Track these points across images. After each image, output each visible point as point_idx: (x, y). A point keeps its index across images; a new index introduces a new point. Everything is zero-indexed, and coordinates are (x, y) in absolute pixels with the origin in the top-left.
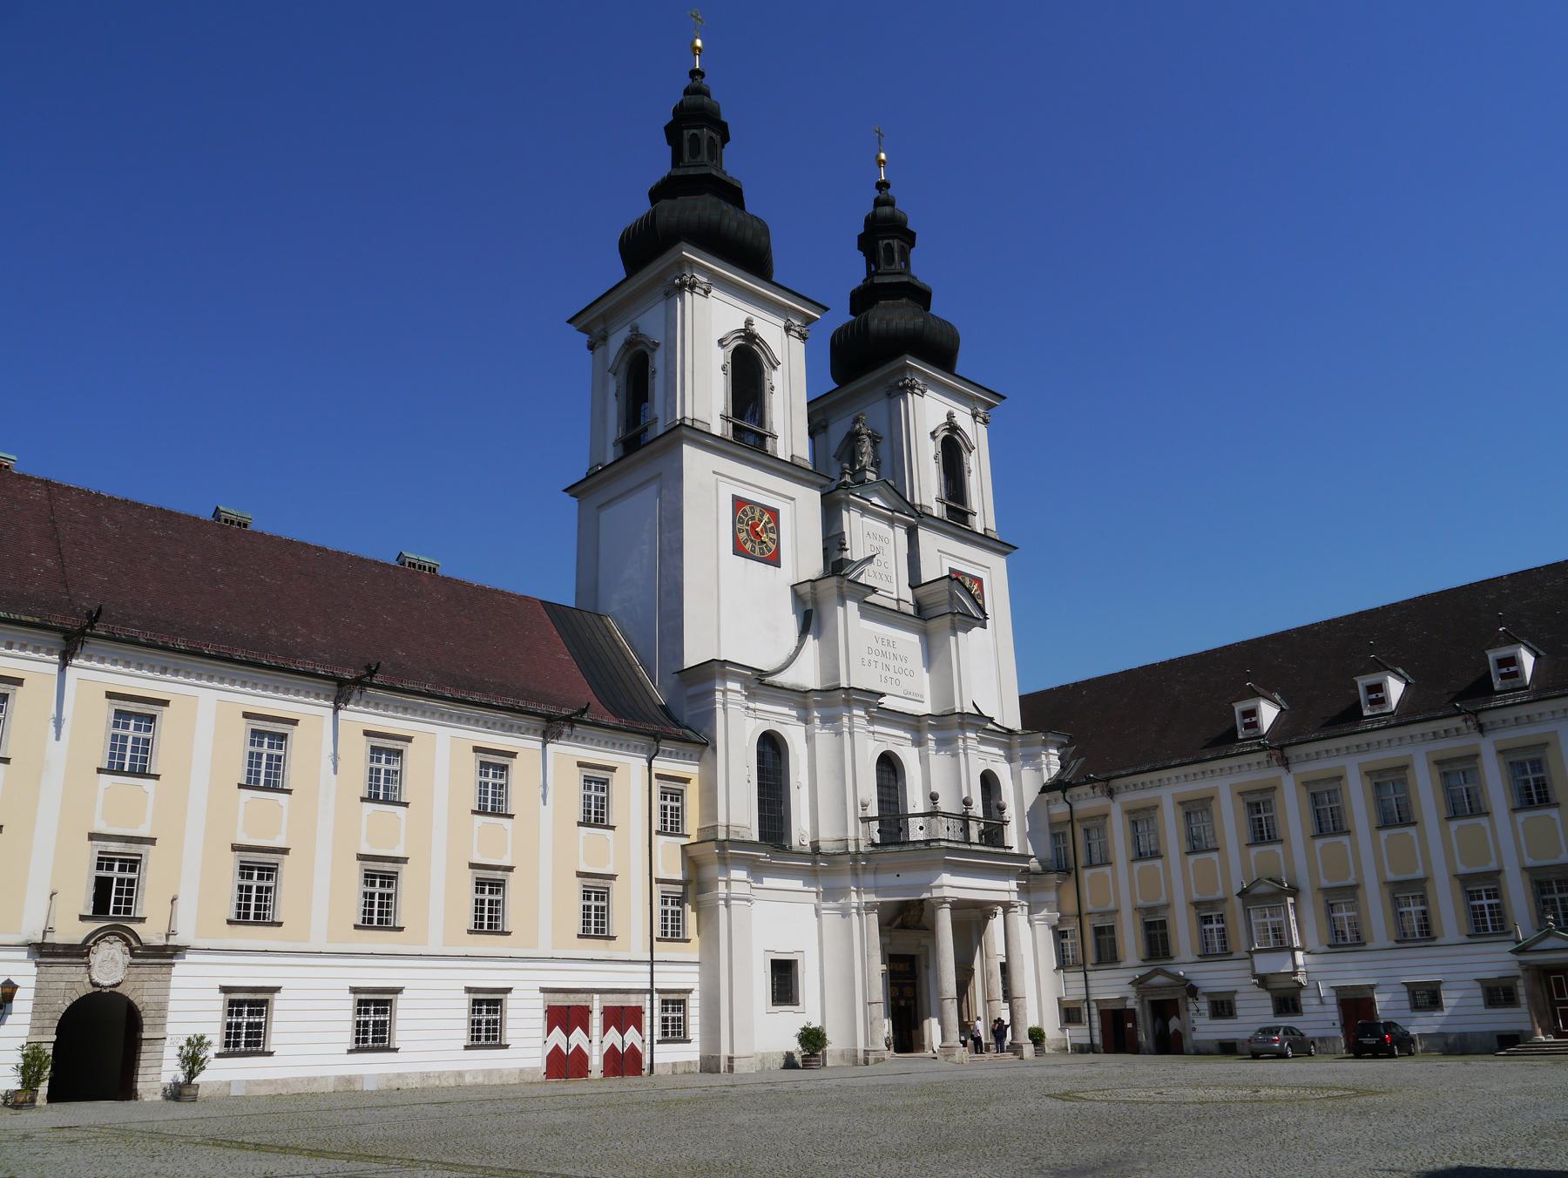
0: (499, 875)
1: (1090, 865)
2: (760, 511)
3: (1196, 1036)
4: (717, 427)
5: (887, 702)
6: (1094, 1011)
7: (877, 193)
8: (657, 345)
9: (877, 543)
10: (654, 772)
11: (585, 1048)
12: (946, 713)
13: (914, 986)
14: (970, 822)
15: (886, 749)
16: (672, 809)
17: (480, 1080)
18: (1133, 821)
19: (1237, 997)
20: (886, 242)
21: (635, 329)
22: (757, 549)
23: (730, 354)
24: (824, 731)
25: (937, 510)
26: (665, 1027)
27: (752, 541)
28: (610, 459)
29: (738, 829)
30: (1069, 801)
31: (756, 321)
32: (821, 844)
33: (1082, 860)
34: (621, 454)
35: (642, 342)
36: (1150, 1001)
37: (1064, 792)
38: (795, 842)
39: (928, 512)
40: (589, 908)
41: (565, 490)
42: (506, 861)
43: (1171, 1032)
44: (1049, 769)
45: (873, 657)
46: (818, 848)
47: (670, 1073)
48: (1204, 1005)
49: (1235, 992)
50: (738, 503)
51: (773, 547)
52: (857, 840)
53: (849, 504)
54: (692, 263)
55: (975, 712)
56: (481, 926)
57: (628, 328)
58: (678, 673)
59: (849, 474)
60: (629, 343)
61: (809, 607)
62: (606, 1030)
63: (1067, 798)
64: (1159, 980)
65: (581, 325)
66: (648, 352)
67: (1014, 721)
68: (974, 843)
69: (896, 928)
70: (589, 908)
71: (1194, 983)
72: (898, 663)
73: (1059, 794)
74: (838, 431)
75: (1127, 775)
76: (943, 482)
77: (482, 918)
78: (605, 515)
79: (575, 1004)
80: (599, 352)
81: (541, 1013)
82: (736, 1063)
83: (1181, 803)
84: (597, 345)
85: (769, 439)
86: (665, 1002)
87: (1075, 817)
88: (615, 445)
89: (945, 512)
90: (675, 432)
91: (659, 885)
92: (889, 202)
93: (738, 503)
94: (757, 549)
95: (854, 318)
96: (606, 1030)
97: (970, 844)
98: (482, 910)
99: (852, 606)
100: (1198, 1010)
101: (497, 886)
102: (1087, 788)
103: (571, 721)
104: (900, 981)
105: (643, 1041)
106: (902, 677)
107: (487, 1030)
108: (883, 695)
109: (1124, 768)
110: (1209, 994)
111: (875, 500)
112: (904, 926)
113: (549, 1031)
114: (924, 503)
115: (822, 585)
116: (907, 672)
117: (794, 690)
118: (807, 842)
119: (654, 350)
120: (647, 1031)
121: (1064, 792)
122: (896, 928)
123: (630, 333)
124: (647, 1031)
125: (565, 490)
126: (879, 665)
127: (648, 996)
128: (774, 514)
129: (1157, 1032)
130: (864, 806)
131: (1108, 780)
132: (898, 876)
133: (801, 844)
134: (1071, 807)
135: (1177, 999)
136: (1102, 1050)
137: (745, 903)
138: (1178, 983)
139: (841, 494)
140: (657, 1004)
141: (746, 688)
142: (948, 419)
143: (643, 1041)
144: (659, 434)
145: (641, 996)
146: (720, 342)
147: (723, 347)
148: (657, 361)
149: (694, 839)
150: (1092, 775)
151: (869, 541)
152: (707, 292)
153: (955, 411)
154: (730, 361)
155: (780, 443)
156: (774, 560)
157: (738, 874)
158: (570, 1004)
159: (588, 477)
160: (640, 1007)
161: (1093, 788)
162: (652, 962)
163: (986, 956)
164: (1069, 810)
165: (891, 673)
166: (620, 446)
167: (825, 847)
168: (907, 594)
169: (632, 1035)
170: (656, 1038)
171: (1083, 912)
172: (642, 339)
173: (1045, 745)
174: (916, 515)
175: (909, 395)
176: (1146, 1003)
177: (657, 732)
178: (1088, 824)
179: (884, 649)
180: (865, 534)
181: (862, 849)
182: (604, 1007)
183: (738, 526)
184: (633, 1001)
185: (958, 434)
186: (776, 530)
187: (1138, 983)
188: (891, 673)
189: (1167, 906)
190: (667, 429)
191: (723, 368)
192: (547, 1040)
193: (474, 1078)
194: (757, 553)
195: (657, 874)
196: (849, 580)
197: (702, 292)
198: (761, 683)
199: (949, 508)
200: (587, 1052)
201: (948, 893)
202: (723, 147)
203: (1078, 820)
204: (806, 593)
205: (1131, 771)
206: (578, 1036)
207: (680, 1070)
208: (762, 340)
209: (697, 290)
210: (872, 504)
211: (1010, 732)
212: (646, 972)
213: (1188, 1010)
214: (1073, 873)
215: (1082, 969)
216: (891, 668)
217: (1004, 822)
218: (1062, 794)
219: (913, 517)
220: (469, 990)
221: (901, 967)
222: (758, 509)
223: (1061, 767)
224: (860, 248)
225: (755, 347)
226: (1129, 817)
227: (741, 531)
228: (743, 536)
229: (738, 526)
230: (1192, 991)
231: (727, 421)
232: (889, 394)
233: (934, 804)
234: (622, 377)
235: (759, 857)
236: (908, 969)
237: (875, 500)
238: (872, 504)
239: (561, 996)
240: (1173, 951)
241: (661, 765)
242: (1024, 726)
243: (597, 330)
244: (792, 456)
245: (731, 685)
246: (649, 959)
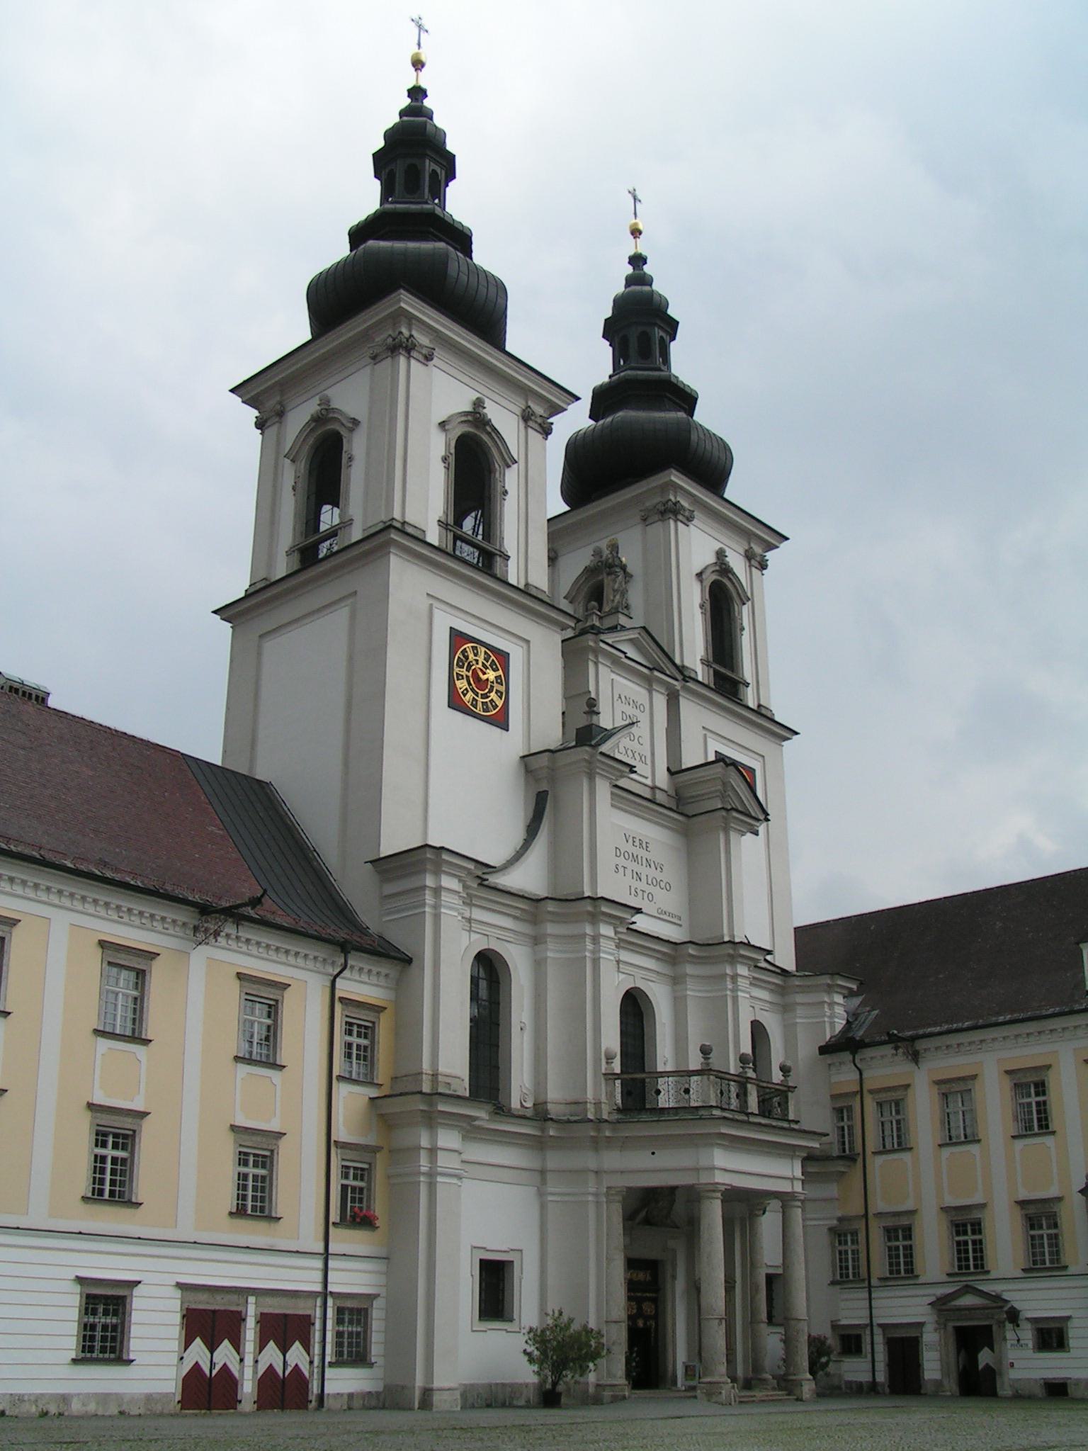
0: (128, 1123)
1: (884, 1151)
2: (486, 653)
3: (1013, 1374)
4: (433, 536)
5: (641, 923)
6: (879, 1338)
7: (630, 270)
8: (356, 422)
9: (630, 710)
10: (338, 994)
11: (234, 1368)
12: (710, 942)
13: (655, 1301)
14: (749, 1086)
15: (632, 986)
16: (358, 1046)
17: (92, 1407)
18: (943, 1094)
19: (1070, 1324)
20: (640, 329)
21: (325, 402)
22: (480, 705)
23: (453, 444)
25: (701, 673)
26: (339, 1345)
27: (473, 690)
28: (281, 572)
29: (448, 1080)
30: (859, 1065)
31: (488, 403)
32: (549, 1106)
33: (871, 1147)
34: (296, 566)
35: (336, 419)
36: (958, 1330)
37: (854, 1053)
38: (515, 1104)
39: (693, 675)
40: (245, 1177)
41: (215, 612)
42: (138, 1105)
43: (980, 1367)
44: (832, 1024)
46: (546, 1112)
47: (345, 1407)
48: (1027, 1335)
49: (1069, 1318)
50: (458, 638)
51: (500, 703)
52: (598, 1104)
53: (597, 652)
55: (746, 941)
56: (101, 1192)
57: (316, 400)
58: (371, 862)
59: (597, 615)
60: (318, 420)
61: (544, 787)
62: (262, 1346)
63: (857, 1061)
64: (968, 1300)
65: (249, 396)
66: (343, 432)
67: (786, 958)
68: (752, 1114)
69: (639, 1224)
70: (245, 1177)
71: (1017, 1305)
72: (652, 872)
73: (847, 1056)
74: (577, 562)
75: (940, 1034)
76: (710, 638)
77: (102, 1181)
78: (269, 645)
79: (222, 1308)
80: (272, 431)
81: (177, 1318)
82: (436, 1398)
83: (1009, 1072)
84: (268, 424)
85: (498, 559)
86: (340, 1311)
87: (866, 1087)
88: (288, 554)
89: (712, 678)
90: (381, 539)
91: (339, 1151)
92: (646, 280)
93: (458, 638)
94: (480, 705)
95: (592, 422)
96: (262, 1346)
97: (748, 1114)
98: (103, 1171)
99: (603, 790)
100: (1018, 1340)
101: (126, 1140)
102: (888, 1050)
103: (234, 914)
104: (639, 1294)
105: (311, 1362)
106: (656, 891)
107: (104, 1339)
108: (639, 911)
109: (935, 1025)
110: (1034, 1321)
111: (632, 653)
112: (648, 1222)
113: (188, 1344)
114: (687, 663)
115: (563, 759)
116: (663, 885)
117: (523, 897)
118: (529, 1104)
119: (351, 430)
120: (317, 1349)
121: (854, 1053)
122: (639, 1224)
123: (319, 408)
124: (317, 1349)
125: (215, 612)
126: (628, 872)
127: (319, 1302)
128: (502, 659)
129: (961, 1367)
130: (609, 1058)
131: (913, 1039)
132: (653, 1153)
133: (522, 1106)
134: (861, 1074)
135: (989, 1328)
136: (887, 1390)
137: (455, 1181)
138: (995, 1305)
139: (590, 641)
140: (330, 1313)
141: (465, 887)
142: (718, 558)
143: (311, 1362)
144: (354, 540)
145: (310, 1302)
146: (442, 425)
147: (445, 430)
148: (357, 447)
149: (385, 1091)
150: (895, 1032)
151: (620, 707)
152: (428, 358)
153: (727, 549)
154: (453, 451)
155: (512, 564)
156: (501, 720)
157: (448, 1138)
158: (217, 1308)
159: (248, 595)
160: (309, 1316)
161: (896, 1048)
162: (326, 1255)
163: (752, 1264)
164: (858, 1077)
165: (642, 885)
166: (296, 556)
167: (553, 1110)
168: (662, 779)
169: (297, 1354)
170: (328, 1359)
171: (871, 1211)
172: (336, 415)
173: (830, 989)
174: (679, 677)
175: (672, 522)
176: (950, 1329)
177: (346, 941)
178: (883, 1097)
179: (637, 851)
180: (616, 697)
181: (605, 1117)
182: (261, 1314)
183: (457, 670)
184: (300, 1308)
185: (730, 579)
186: (504, 679)
187: (940, 1305)
188: (642, 885)
189: (983, 1206)
190: (367, 534)
191: (445, 459)
192: (185, 1355)
193: (84, 1405)
194: (479, 710)
195: (333, 1138)
196: (602, 754)
198: (482, 882)
199: (716, 673)
200: (236, 1374)
201: (720, 1178)
202: (447, 186)
203: (871, 1092)
204: (541, 768)
205: (945, 1027)
206: (225, 1352)
208: (495, 429)
209: (414, 354)
210: (627, 657)
211: (784, 973)
212: (317, 1269)
213: (1005, 1339)
214: (860, 1160)
215: (866, 1284)
216: (644, 878)
217: (789, 1087)
218: (851, 1057)
219: (677, 680)
220: (80, 1280)
221: (641, 1276)
222: (483, 649)
223: (848, 1022)
224: (607, 335)
225: (485, 438)
226: (938, 1089)
227: (460, 677)
228: (461, 685)
229: (457, 670)
230: (1013, 1316)
231: (447, 529)
232: (644, 520)
233: (706, 1059)
234: (303, 465)
235: (476, 1118)
236: (649, 1278)
237: (632, 653)
238: (627, 657)
239: (204, 1297)
240: (989, 1264)
242: (797, 971)
243: (271, 403)
244: (527, 585)
245: (448, 882)
246: (321, 1250)
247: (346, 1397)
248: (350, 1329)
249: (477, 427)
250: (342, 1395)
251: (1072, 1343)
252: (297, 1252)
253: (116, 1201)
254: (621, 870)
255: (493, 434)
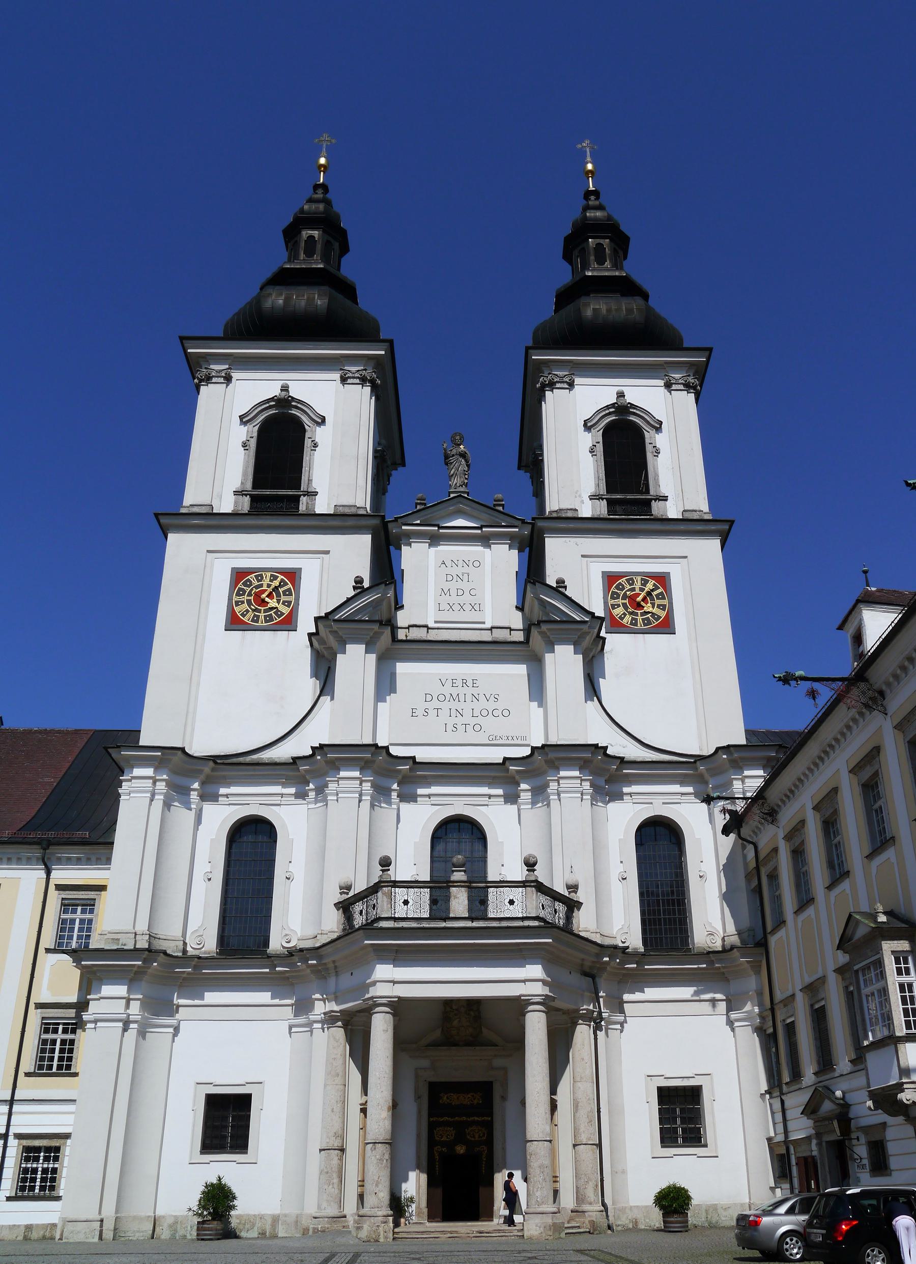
24: (319, 805)
45: (435, 704)
47: (21, 1238)
54: (207, 358)
191: (244, 445)
197: (222, 380)
207: (35, 1235)
208: (300, 401)
241: (61, 875)
247: (23, 1229)
248: (45, 1166)
249: (283, 407)
250: (19, 1226)
251: (893, 1163)
252: (33, 1100)
253: (64, 1073)
254: (432, 713)
255: (299, 405)
